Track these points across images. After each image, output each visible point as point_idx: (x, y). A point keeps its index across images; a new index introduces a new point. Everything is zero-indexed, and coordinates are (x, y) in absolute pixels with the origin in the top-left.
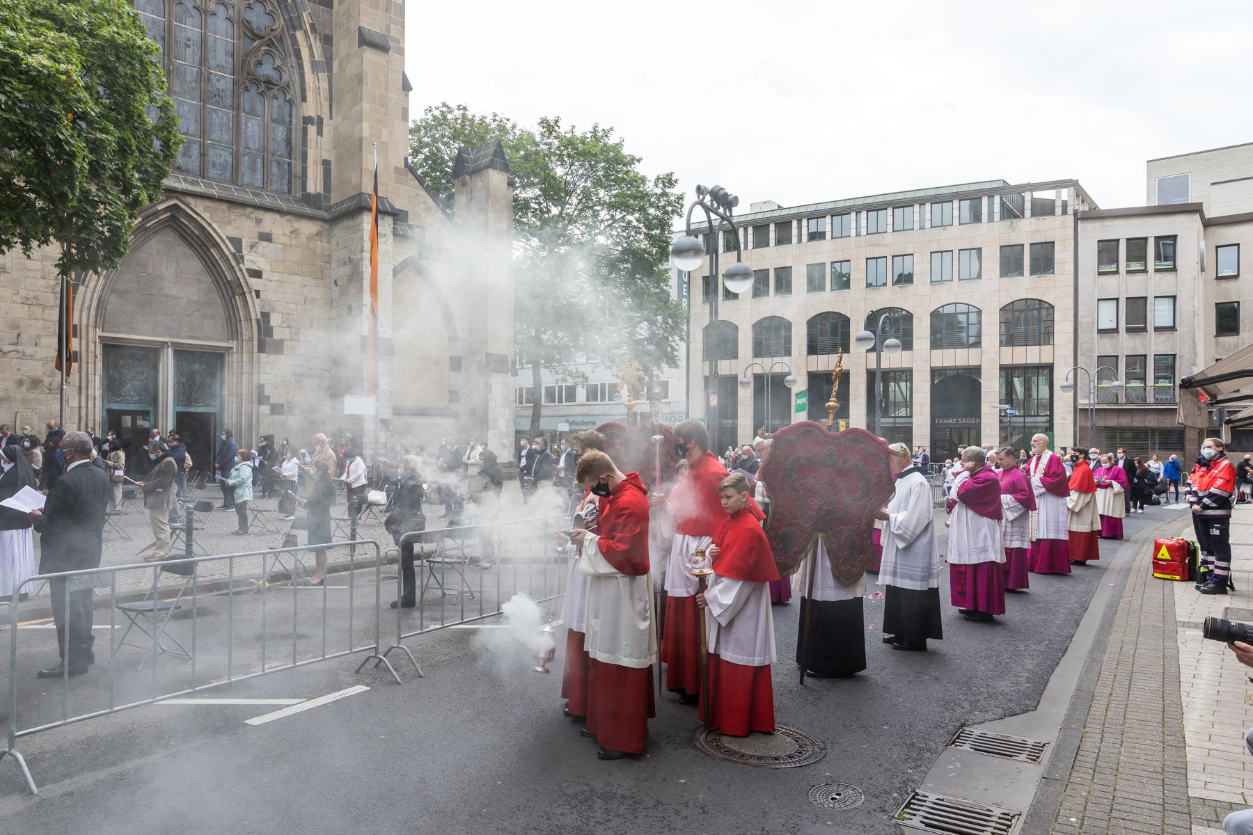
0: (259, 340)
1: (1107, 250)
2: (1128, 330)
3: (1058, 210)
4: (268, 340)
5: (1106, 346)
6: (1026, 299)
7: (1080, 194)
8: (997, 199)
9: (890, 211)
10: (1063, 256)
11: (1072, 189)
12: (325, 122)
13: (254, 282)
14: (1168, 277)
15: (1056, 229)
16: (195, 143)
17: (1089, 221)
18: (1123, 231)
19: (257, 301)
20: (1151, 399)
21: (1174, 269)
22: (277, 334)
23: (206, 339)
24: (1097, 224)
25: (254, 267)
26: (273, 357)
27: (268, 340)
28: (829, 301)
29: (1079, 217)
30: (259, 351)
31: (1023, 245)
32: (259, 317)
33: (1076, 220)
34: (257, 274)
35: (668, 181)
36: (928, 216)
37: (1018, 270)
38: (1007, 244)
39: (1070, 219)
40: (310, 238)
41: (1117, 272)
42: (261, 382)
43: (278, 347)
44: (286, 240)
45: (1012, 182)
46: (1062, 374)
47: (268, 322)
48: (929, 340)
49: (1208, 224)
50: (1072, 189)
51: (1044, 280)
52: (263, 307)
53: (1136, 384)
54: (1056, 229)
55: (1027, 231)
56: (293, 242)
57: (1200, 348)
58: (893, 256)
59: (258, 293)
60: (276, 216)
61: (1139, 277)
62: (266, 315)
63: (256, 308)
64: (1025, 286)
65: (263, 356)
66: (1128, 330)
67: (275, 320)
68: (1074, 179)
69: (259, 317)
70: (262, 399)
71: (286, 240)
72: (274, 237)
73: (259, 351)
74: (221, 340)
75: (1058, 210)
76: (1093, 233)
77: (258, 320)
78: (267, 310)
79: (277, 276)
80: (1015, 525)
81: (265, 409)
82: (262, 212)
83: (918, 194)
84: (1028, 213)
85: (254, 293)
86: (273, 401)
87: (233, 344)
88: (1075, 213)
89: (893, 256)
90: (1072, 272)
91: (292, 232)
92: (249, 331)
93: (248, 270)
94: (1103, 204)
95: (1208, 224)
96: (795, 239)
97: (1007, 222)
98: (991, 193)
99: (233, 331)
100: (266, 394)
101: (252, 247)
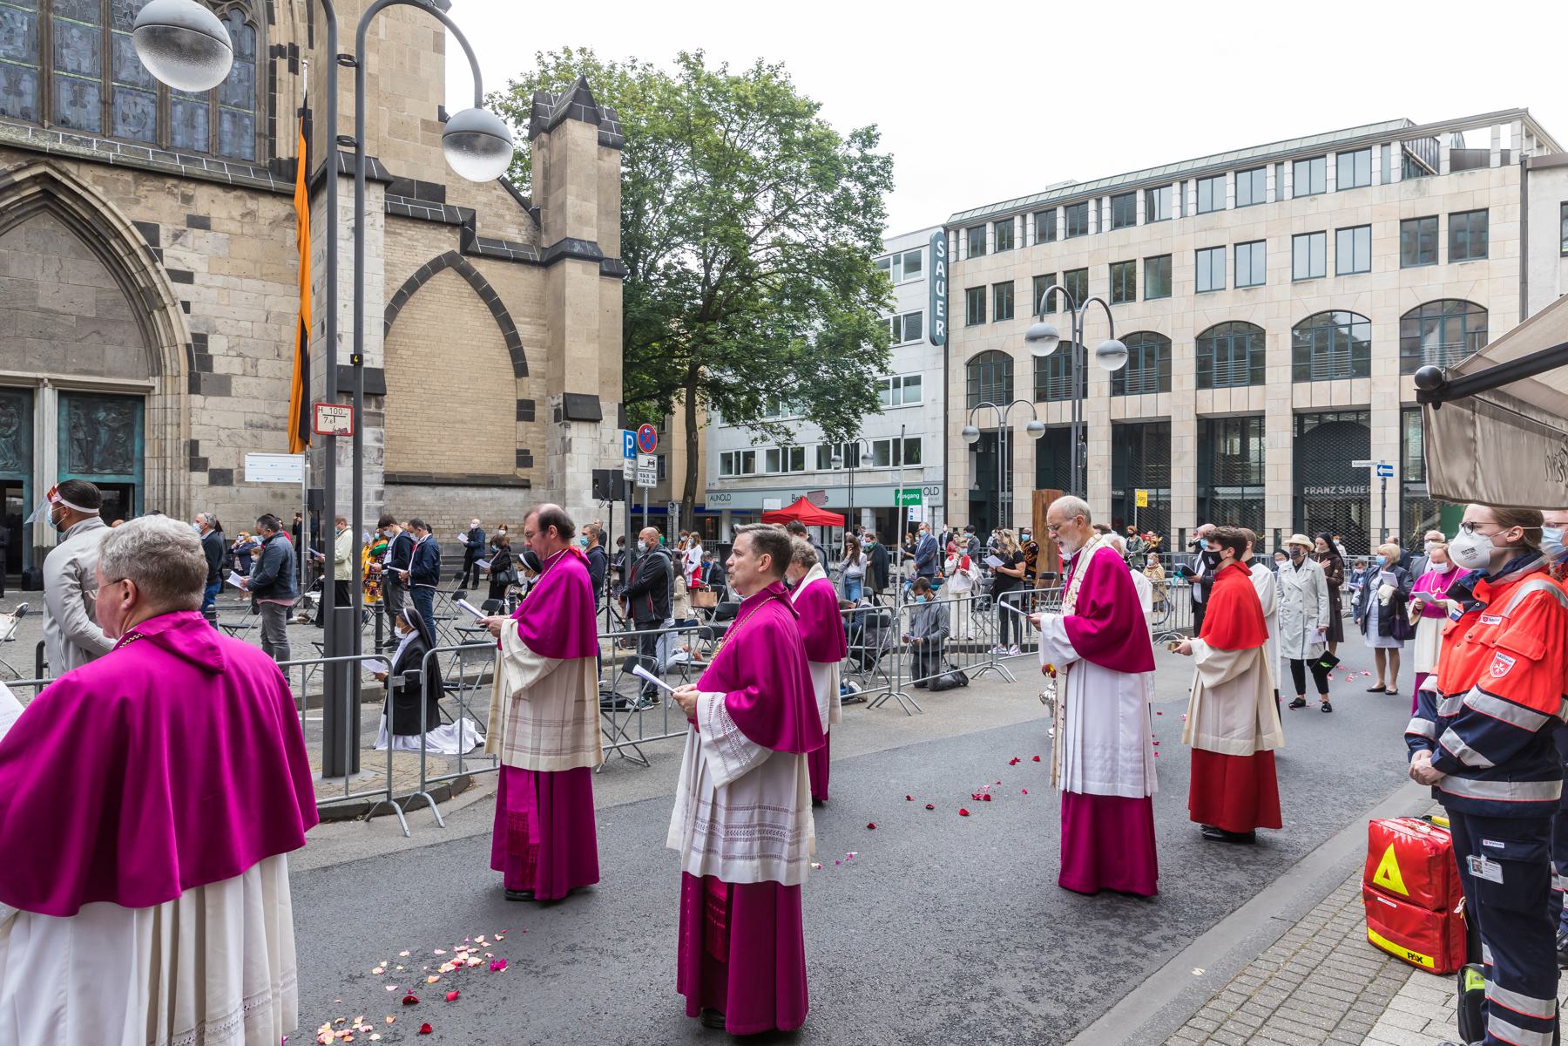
0: (190, 375)
3: (1495, 159)
4: (203, 374)
6: (1443, 300)
7: (1532, 131)
8: (1396, 148)
9: (1230, 176)
10: (1502, 232)
11: (1518, 124)
12: (302, 52)
13: (180, 290)
16: (93, 86)
17: (1547, 172)
19: (185, 318)
22: (220, 367)
23: (111, 374)
25: (179, 267)
26: (212, 400)
27: (203, 374)
28: (1137, 316)
29: (1529, 166)
30: (191, 392)
31: (1437, 217)
32: (190, 341)
33: (1525, 171)
34: (186, 277)
35: (868, 137)
36: (1288, 181)
37: (1430, 256)
38: (1412, 216)
39: (1514, 171)
40: (274, 223)
42: (194, 437)
43: (223, 386)
44: (234, 227)
45: (1420, 120)
47: (205, 348)
48: (1290, 369)
50: (1518, 124)
51: (1473, 267)
52: (193, 326)
56: (247, 230)
58: (1236, 245)
59: (186, 306)
60: (218, 192)
62: (200, 340)
63: (182, 328)
65: (197, 400)
67: (215, 346)
68: (1522, 107)
69: (190, 341)
70: (196, 463)
71: (234, 227)
72: (214, 224)
73: (191, 392)
74: (137, 378)
75: (1495, 159)
77: (188, 346)
78: (202, 331)
79: (219, 281)
80: (746, 798)
81: (201, 478)
82: (192, 186)
83: (1274, 149)
84: (1445, 166)
85: (179, 306)
86: (213, 465)
87: (155, 382)
88: (1523, 163)
89: (1236, 245)
90: (1518, 254)
91: (243, 216)
93: (169, 272)
96: (1092, 228)
97: (1412, 183)
100: (202, 454)
101: (176, 236)
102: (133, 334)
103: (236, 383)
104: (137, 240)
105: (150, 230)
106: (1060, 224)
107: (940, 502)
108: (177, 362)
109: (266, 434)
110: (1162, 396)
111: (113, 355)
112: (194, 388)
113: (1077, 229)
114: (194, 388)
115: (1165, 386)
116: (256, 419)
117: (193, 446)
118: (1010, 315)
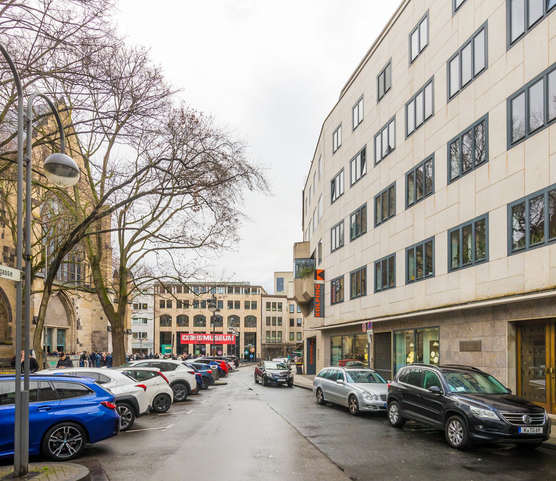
1: (268, 304)
2: (273, 325)
5: (267, 328)
10: (259, 305)
14: (280, 312)
15: (257, 298)
18: (272, 300)
20: (277, 342)
21: (281, 311)
24: (266, 298)
33: (262, 296)
39: (260, 296)
41: (270, 310)
43: (81, 329)
46: (259, 335)
49: (288, 299)
51: (255, 311)
53: (274, 338)
54: (257, 298)
55: (251, 298)
57: (287, 330)
61: (275, 312)
62: (79, 319)
64: (250, 312)
66: (273, 325)
67: (81, 321)
76: (265, 300)
92: (74, 324)
94: (269, 294)
95: (288, 299)
97: (246, 295)
98: (243, 286)
99: (69, 323)
102: (66, 318)
103: (83, 328)
104: (71, 301)
105: (73, 299)
106: (183, 290)
107: (153, 347)
108: (74, 324)
109: (86, 337)
110: (204, 327)
111: (64, 321)
112: (78, 329)
113: (186, 291)
114: (78, 329)
115: (204, 325)
116: (85, 334)
117: (78, 339)
118: (171, 307)
